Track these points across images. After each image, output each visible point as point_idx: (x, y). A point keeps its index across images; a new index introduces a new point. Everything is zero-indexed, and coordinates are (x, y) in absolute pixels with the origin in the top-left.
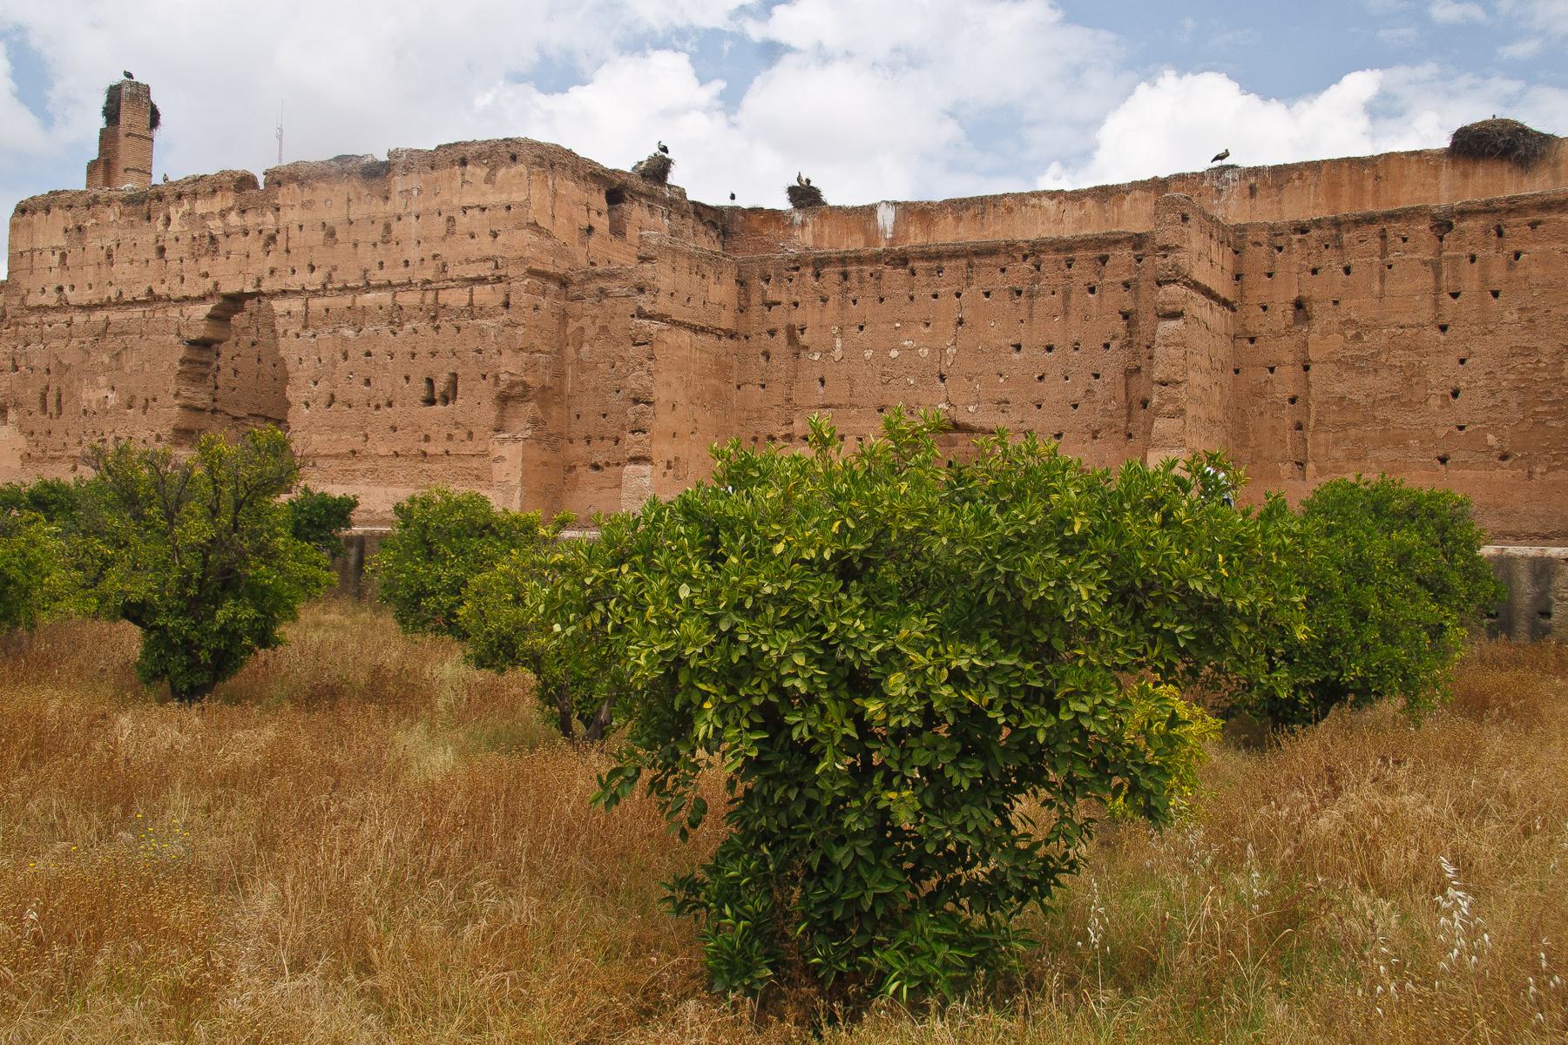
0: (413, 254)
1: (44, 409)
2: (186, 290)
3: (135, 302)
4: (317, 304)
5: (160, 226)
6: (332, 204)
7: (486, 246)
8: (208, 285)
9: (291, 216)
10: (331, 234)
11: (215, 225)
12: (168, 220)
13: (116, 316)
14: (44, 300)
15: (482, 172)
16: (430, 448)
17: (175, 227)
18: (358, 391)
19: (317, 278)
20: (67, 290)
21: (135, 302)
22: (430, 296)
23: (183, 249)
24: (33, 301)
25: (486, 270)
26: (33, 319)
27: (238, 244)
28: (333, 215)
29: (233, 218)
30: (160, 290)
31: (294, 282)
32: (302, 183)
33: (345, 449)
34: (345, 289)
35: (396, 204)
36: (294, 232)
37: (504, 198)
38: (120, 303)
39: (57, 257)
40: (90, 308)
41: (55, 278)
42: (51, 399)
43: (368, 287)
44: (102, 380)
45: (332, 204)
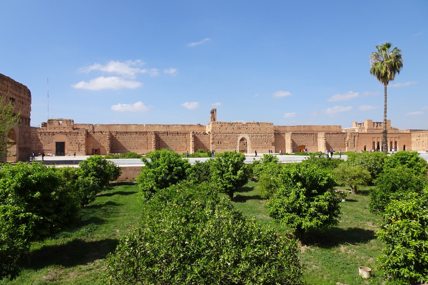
0: (263, 131)
1: (218, 143)
2: (237, 132)
3: (230, 133)
4: (253, 135)
5: (233, 126)
6: (254, 126)
7: (270, 131)
8: (240, 132)
9: (249, 127)
10: (254, 129)
11: (240, 127)
12: (234, 126)
13: (228, 135)
14: (217, 132)
15: (269, 125)
16: (266, 147)
17: (235, 126)
18: (258, 142)
19: (253, 132)
20: (221, 131)
21: (230, 133)
22: (265, 135)
23: (236, 128)
24: (216, 132)
25: (270, 133)
26: (216, 134)
27: (243, 129)
28: (254, 127)
29: (243, 126)
30: (233, 132)
31: (250, 133)
32: (251, 124)
33: (257, 147)
34: (256, 133)
35: (261, 127)
36: (250, 128)
37: (271, 127)
38: (228, 133)
39: (219, 128)
40: (224, 133)
41: (219, 130)
42: (219, 143)
43: (258, 133)
44: (227, 141)
45: (254, 126)
